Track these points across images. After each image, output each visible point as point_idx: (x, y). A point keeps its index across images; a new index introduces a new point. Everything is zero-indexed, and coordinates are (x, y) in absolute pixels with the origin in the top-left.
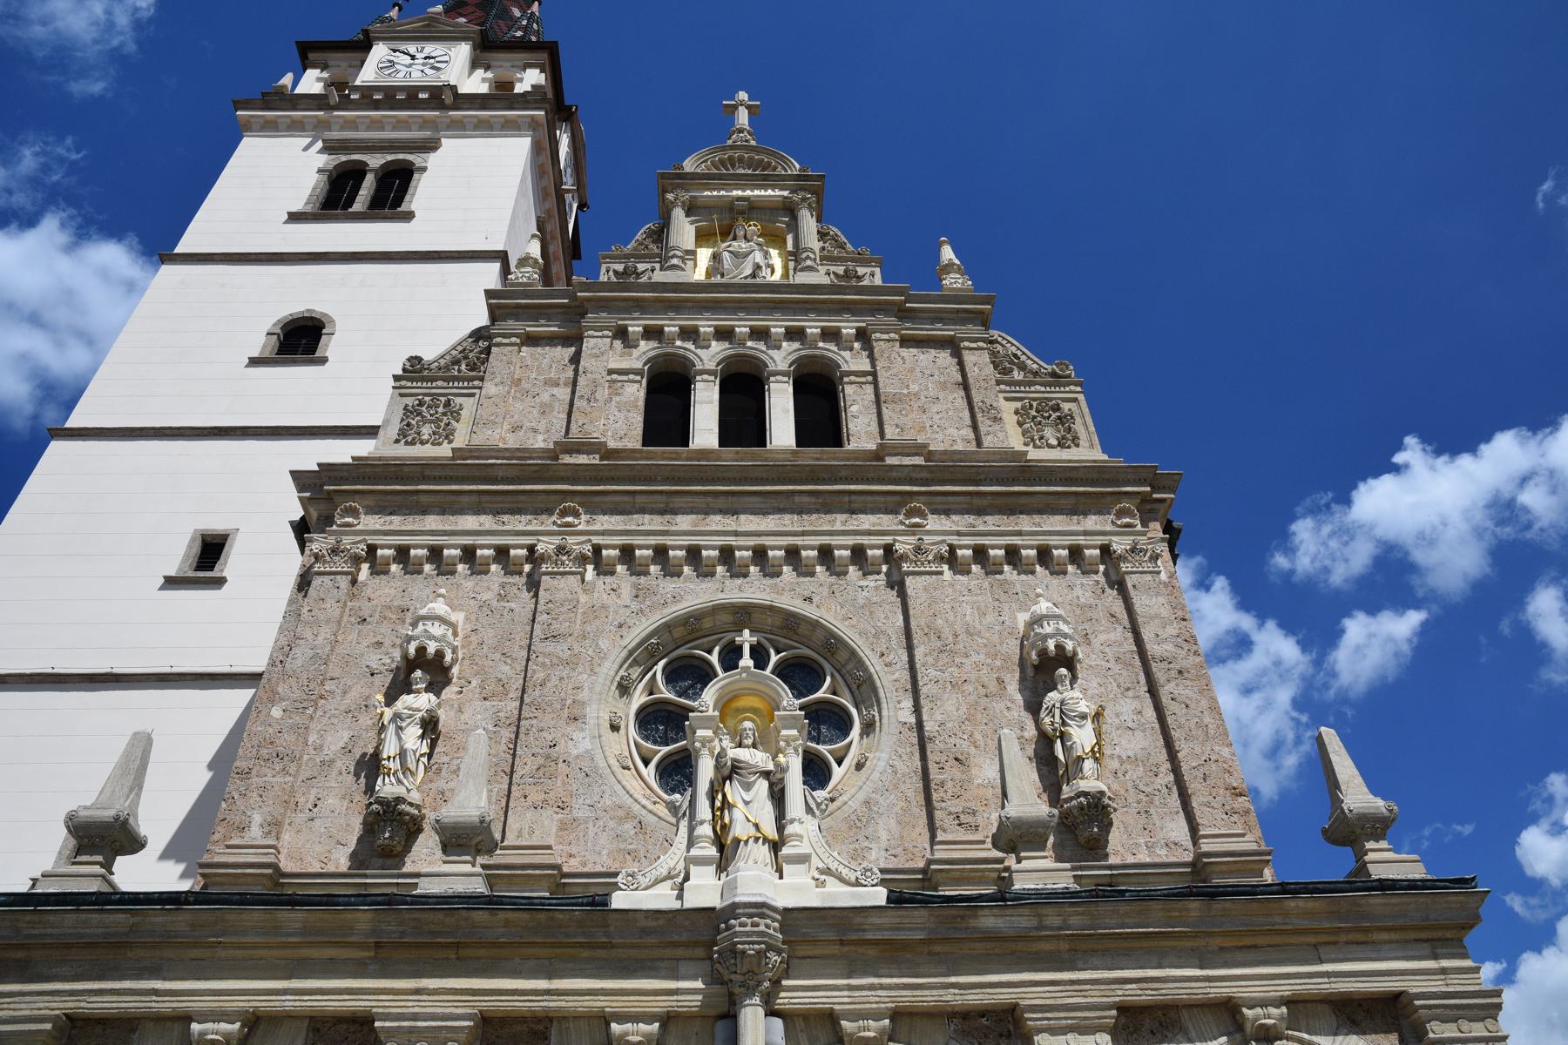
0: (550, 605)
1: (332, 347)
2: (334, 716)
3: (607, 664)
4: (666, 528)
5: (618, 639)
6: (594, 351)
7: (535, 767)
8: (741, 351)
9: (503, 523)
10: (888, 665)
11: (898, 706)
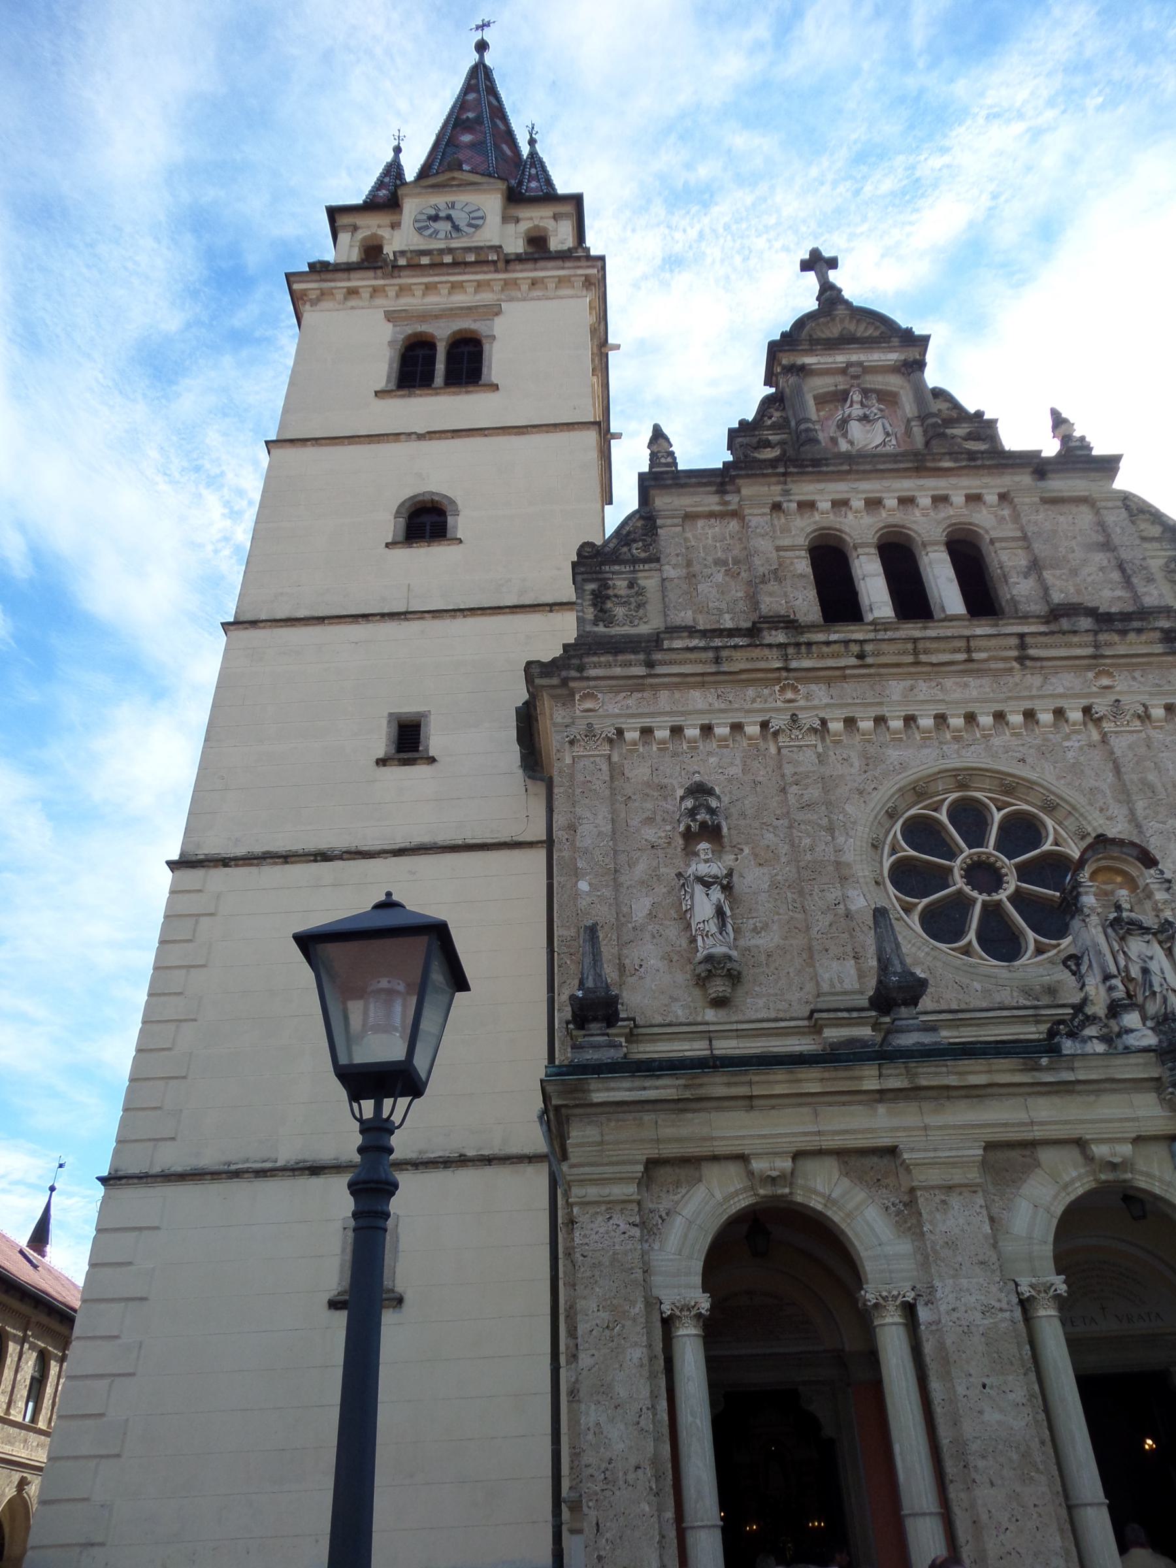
0: (796, 777)
1: (461, 524)
2: (631, 886)
4: (879, 700)
5: (863, 805)
7: (827, 923)
8: (891, 520)
9: (730, 702)
10: (1109, 818)
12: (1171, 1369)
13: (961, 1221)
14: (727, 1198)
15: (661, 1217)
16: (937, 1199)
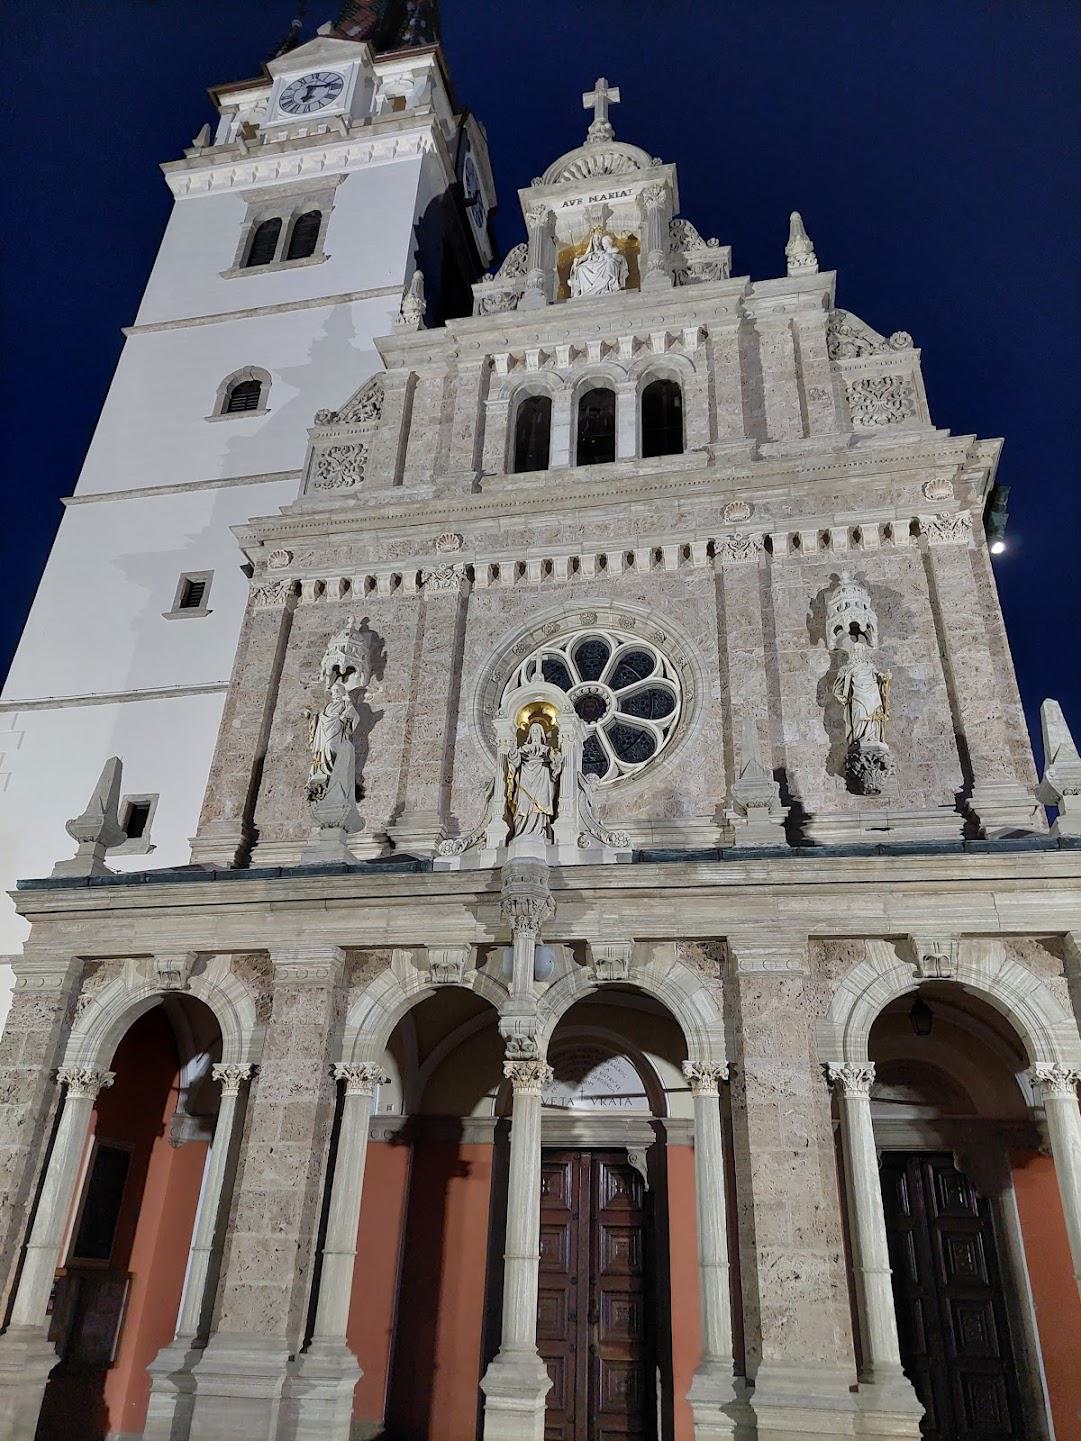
3: (481, 666)
6: (467, 387)
11: (712, 684)
12: (628, 1148)
13: (302, 1013)
14: (137, 988)
15: (83, 1004)
16: (289, 995)
